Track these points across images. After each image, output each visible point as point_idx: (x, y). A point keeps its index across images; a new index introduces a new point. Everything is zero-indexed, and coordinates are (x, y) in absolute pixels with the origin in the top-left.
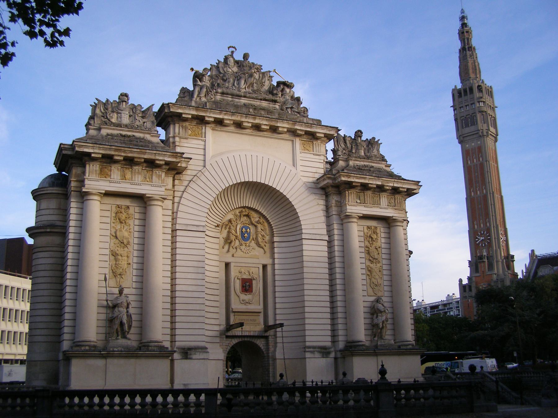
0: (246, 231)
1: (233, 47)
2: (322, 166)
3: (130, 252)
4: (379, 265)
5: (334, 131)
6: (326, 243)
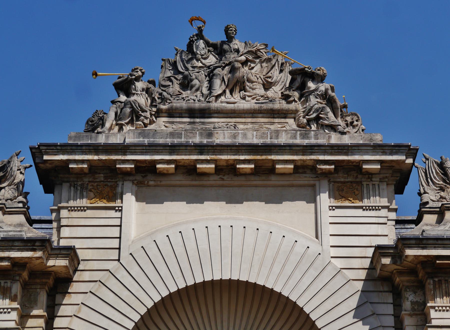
1: (198, 19)
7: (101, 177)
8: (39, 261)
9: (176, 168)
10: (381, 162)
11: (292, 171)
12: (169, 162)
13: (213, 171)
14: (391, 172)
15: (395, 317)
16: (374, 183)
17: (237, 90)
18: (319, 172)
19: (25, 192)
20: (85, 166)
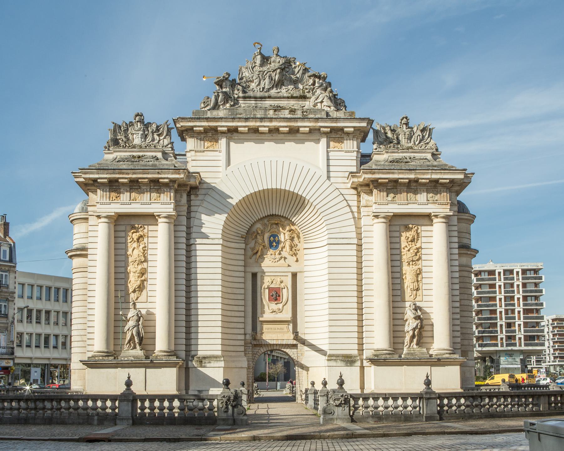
0: (274, 239)
2: (354, 163)
3: (145, 269)
4: (415, 268)
5: (365, 122)
6: (355, 247)
7: (210, 134)
8: (182, 179)
9: (249, 129)
10: (354, 127)
11: (308, 132)
12: (245, 127)
13: (268, 132)
14: (359, 132)
15: (358, 207)
16: (350, 138)
17: (280, 85)
18: (322, 132)
19: (172, 142)
20: (202, 129)
